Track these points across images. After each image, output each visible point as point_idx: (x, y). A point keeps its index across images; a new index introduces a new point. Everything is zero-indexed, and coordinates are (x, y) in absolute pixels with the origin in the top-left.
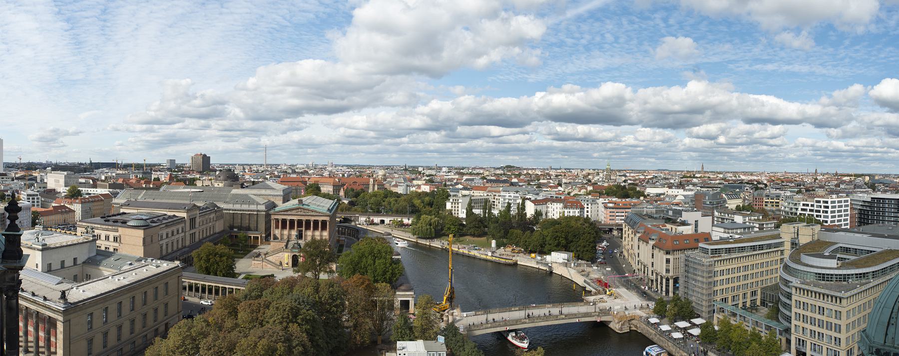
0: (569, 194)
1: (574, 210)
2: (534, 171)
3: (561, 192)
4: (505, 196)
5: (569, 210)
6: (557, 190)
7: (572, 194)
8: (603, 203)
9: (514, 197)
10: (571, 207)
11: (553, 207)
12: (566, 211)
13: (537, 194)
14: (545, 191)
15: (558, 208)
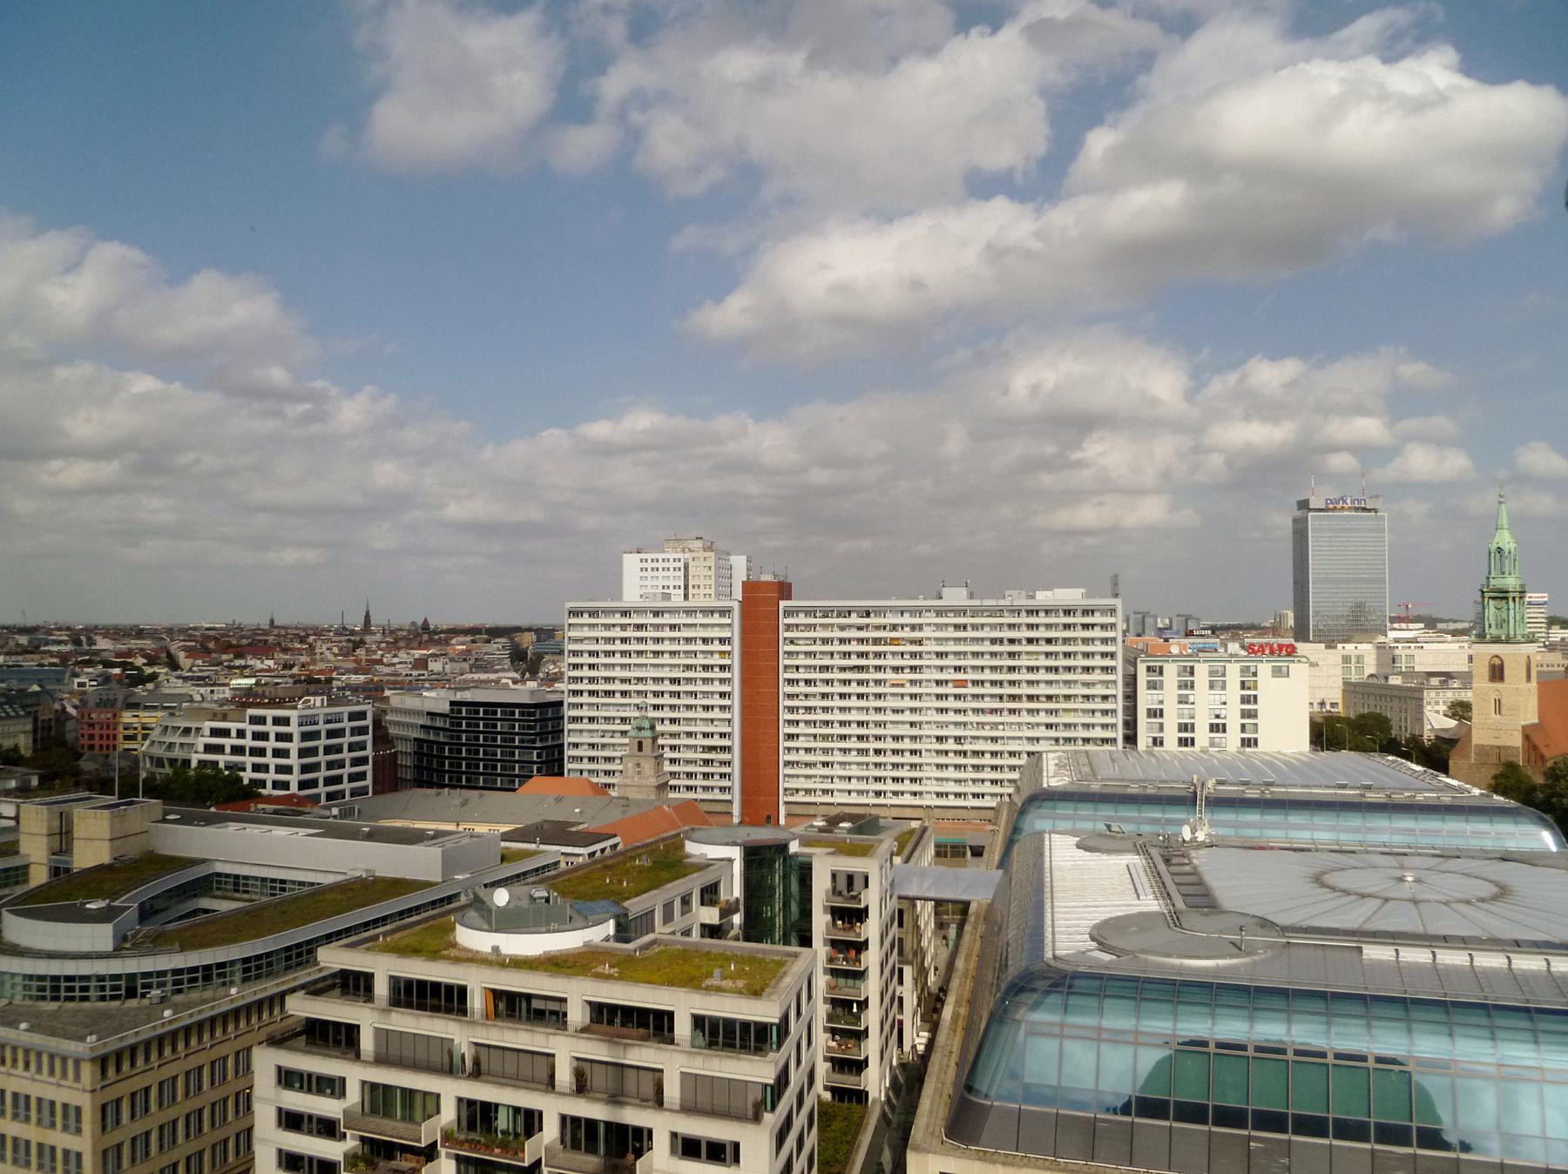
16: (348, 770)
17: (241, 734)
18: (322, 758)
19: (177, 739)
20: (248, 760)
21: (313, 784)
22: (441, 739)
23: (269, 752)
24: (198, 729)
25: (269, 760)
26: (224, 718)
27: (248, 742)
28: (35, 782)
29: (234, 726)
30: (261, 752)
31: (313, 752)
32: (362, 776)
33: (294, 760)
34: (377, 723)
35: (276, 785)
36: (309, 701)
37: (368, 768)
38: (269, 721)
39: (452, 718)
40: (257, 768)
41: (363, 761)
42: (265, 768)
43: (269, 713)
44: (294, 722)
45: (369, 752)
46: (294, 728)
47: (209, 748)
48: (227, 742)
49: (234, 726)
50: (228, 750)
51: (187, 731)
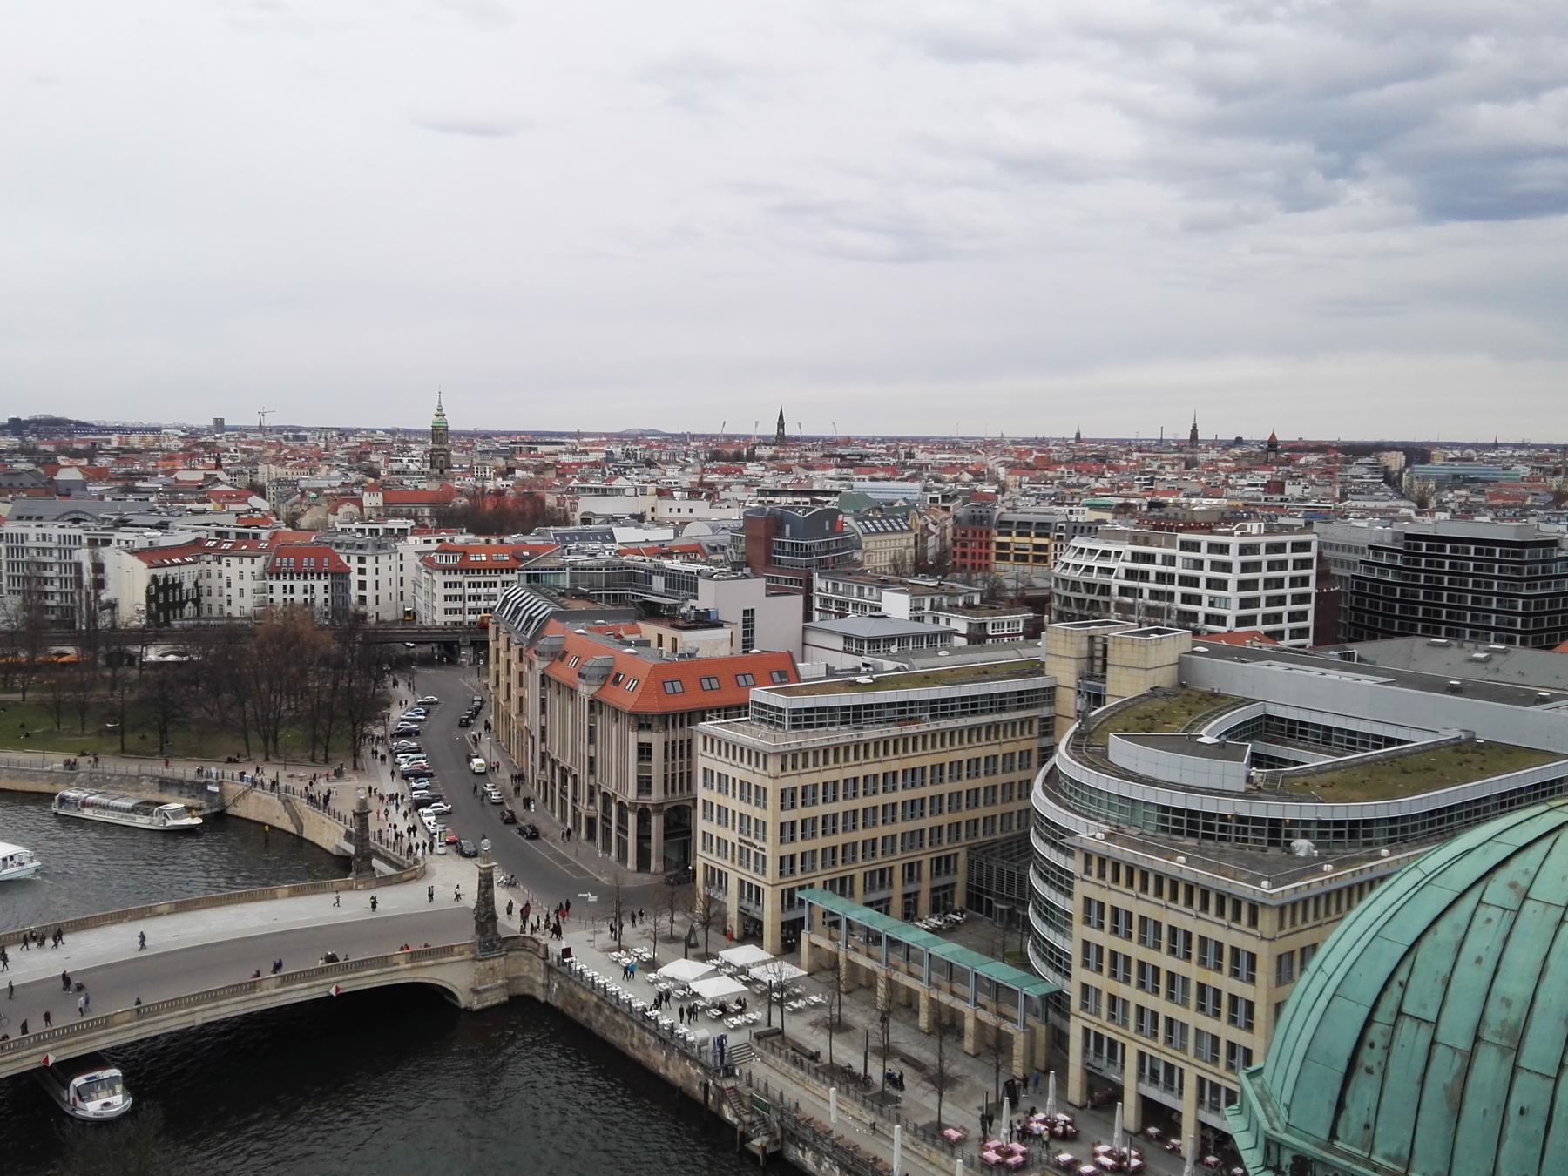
0: (292, 521)
1: (308, 583)
2: (150, 437)
3: (257, 515)
4: (24, 537)
5: (288, 583)
6: (244, 507)
7: (304, 522)
8: (419, 553)
9: (65, 539)
10: (298, 572)
11: (226, 572)
12: (278, 585)
13: (162, 526)
14: (195, 513)
15: (247, 576)
16: (1289, 607)
17: (1170, 561)
18: (1262, 593)
19: (1096, 563)
20: (1178, 590)
21: (1250, 620)
22: (1389, 579)
23: (1203, 583)
24: (1118, 554)
25: (1201, 590)
26: (1146, 542)
27: (1178, 570)
28: (977, 601)
29: (1158, 551)
30: (1194, 582)
31: (1252, 585)
32: (1303, 615)
33: (1232, 593)
34: (1320, 555)
35: (1209, 619)
36: (1245, 527)
37: (1310, 607)
38: (1204, 547)
39: (1406, 554)
40: (1187, 599)
41: (1304, 598)
42: (1197, 600)
43: (1205, 539)
44: (1234, 550)
45: (1311, 588)
46: (1233, 557)
47: (1130, 574)
48: (1152, 569)
49: (1158, 551)
50: (1152, 577)
51: (1106, 554)
